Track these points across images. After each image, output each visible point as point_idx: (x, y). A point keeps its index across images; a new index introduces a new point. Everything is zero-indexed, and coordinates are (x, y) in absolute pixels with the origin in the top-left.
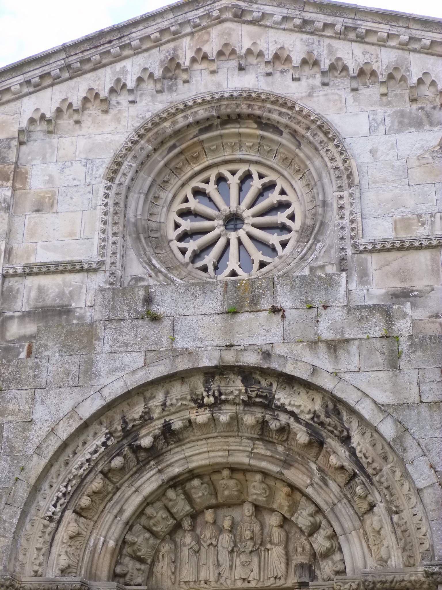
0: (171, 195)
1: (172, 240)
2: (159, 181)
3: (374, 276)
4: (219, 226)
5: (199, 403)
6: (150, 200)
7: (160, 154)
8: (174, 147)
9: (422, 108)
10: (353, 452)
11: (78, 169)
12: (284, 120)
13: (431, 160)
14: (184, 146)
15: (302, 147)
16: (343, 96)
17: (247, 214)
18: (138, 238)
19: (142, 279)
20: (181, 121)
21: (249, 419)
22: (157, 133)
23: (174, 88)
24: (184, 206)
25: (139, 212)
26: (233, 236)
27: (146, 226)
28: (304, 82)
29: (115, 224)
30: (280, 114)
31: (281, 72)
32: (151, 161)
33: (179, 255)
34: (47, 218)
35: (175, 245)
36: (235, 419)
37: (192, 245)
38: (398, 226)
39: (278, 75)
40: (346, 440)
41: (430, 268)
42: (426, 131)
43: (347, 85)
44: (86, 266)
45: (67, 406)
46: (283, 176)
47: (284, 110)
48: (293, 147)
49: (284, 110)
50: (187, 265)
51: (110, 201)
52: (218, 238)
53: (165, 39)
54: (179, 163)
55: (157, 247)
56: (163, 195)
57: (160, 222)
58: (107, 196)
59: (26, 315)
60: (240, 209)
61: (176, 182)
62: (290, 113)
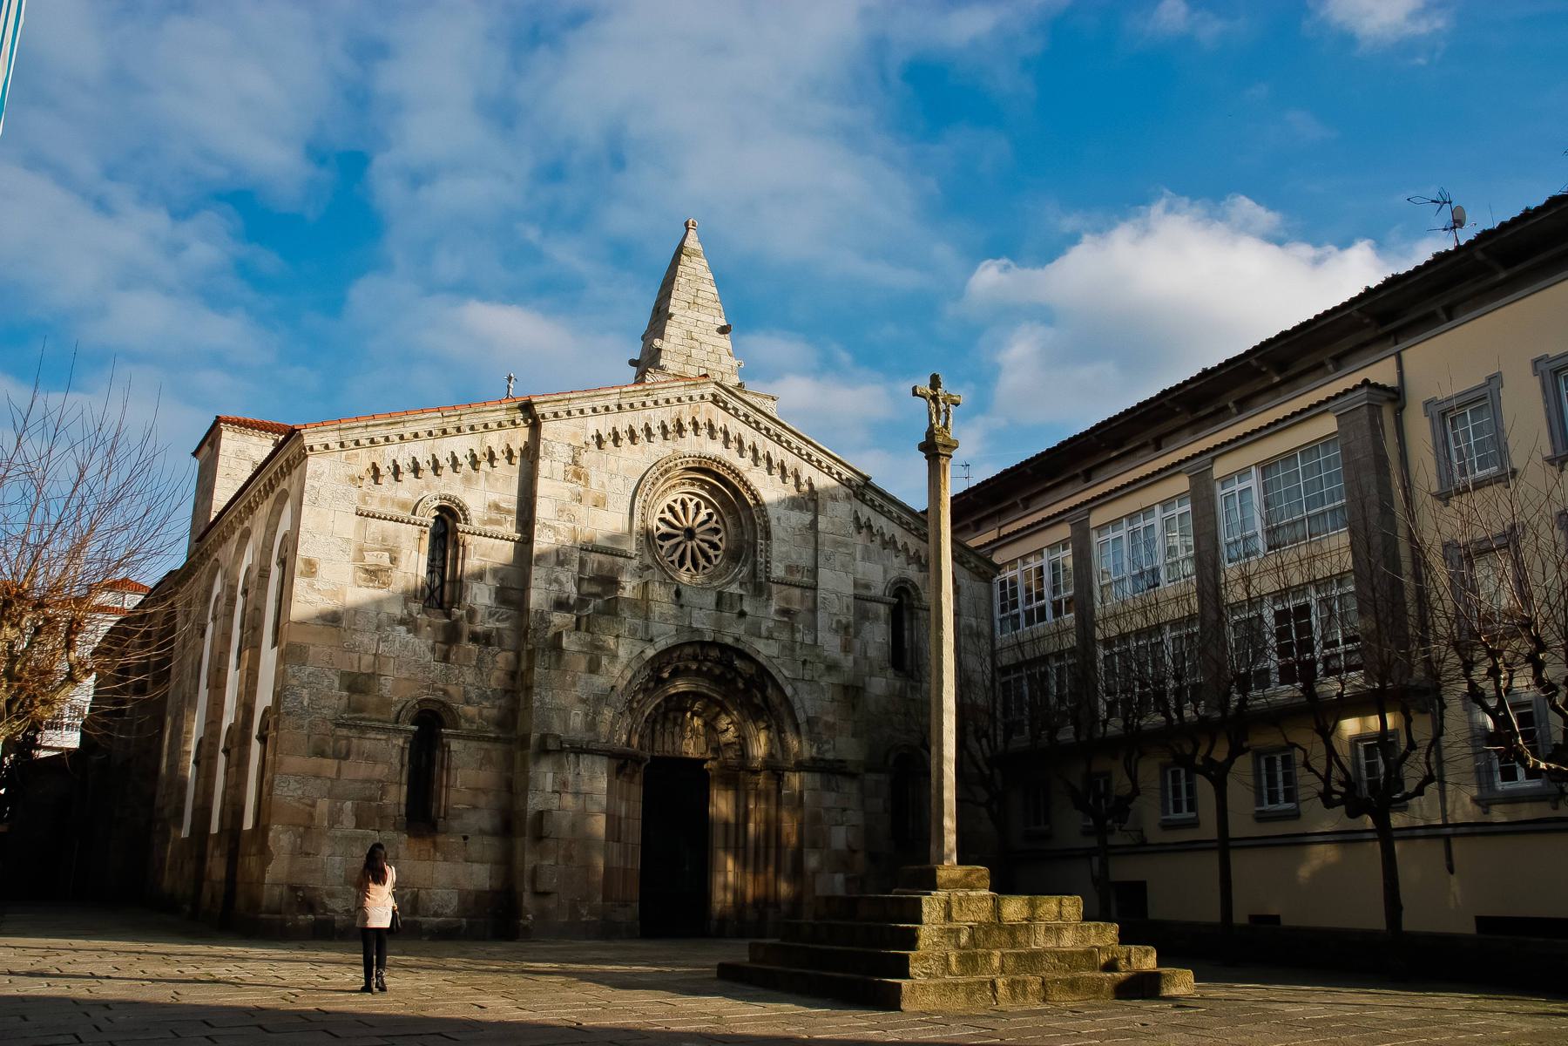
3: (775, 597)
5: (695, 658)
10: (765, 699)
11: (619, 480)
17: (698, 531)
21: (717, 672)
34: (599, 512)
36: (709, 669)
37: (667, 544)
40: (763, 691)
45: (637, 650)
52: (679, 544)
59: (590, 580)
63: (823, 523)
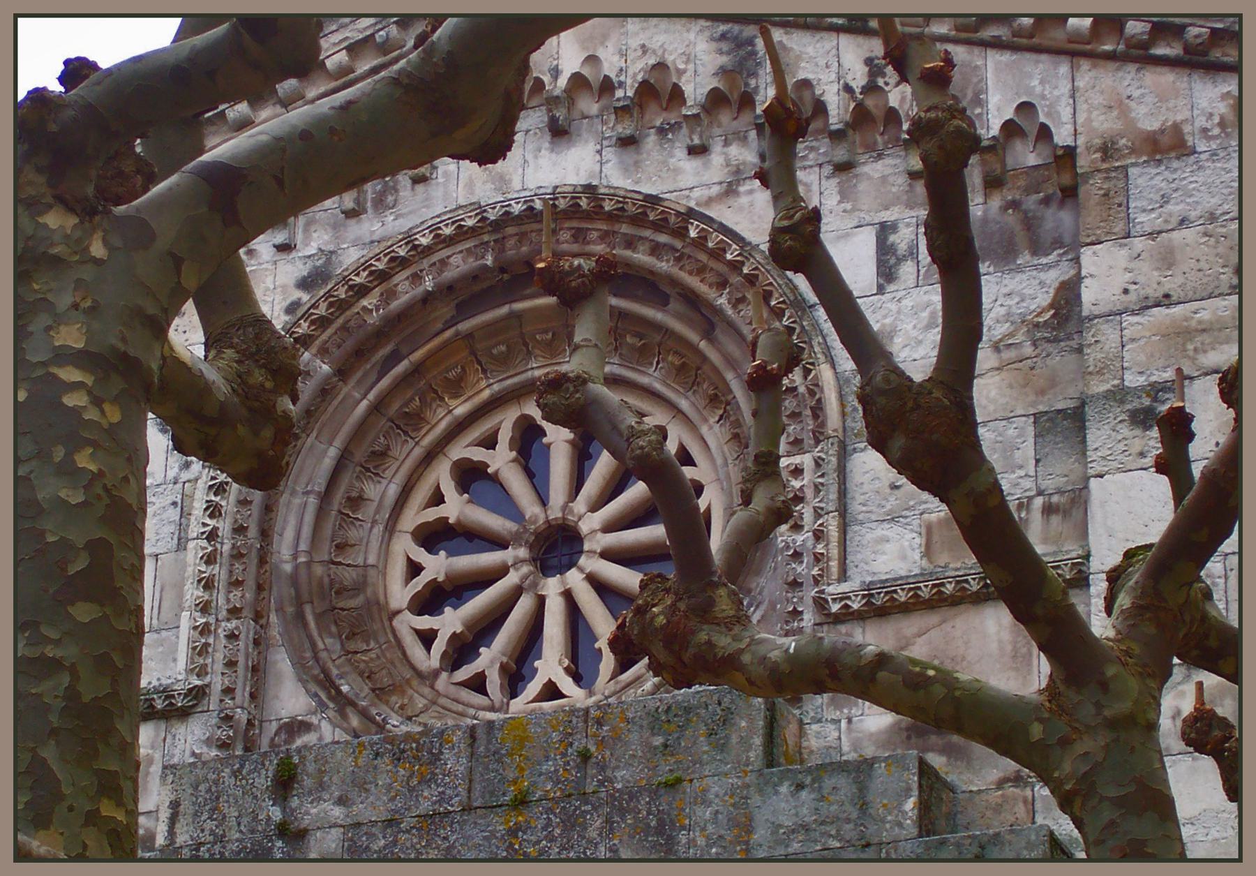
0: (393, 490)
1: (399, 612)
2: (360, 455)
4: (517, 562)
6: (336, 507)
7: (359, 382)
8: (395, 358)
9: (1014, 205)
12: (664, 266)
13: (1028, 350)
14: (418, 355)
15: (718, 332)
16: (815, 188)
17: (589, 523)
18: (300, 616)
19: (305, 727)
20: (405, 291)
22: (344, 328)
23: (390, 199)
24: (432, 514)
25: (303, 546)
26: (552, 587)
27: (326, 580)
28: (716, 158)
29: (238, 583)
30: (656, 250)
31: (662, 131)
32: (336, 402)
33: (416, 651)
35: (409, 623)
37: (450, 622)
38: (935, 538)
39: (651, 140)
41: (1009, 648)
42: (1019, 270)
43: (825, 154)
44: (159, 704)
46: (680, 411)
47: (663, 238)
48: (693, 336)
49: (663, 238)
50: (436, 674)
51: (224, 526)
53: (363, 67)
54: (412, 399)
55: (352, 636)
56: (372, 490)
57: (366, 566)
58: (214, 511)
60: (571, 512)
61: (407, 453)
62: (678, 244)
63: (1105, 274)
